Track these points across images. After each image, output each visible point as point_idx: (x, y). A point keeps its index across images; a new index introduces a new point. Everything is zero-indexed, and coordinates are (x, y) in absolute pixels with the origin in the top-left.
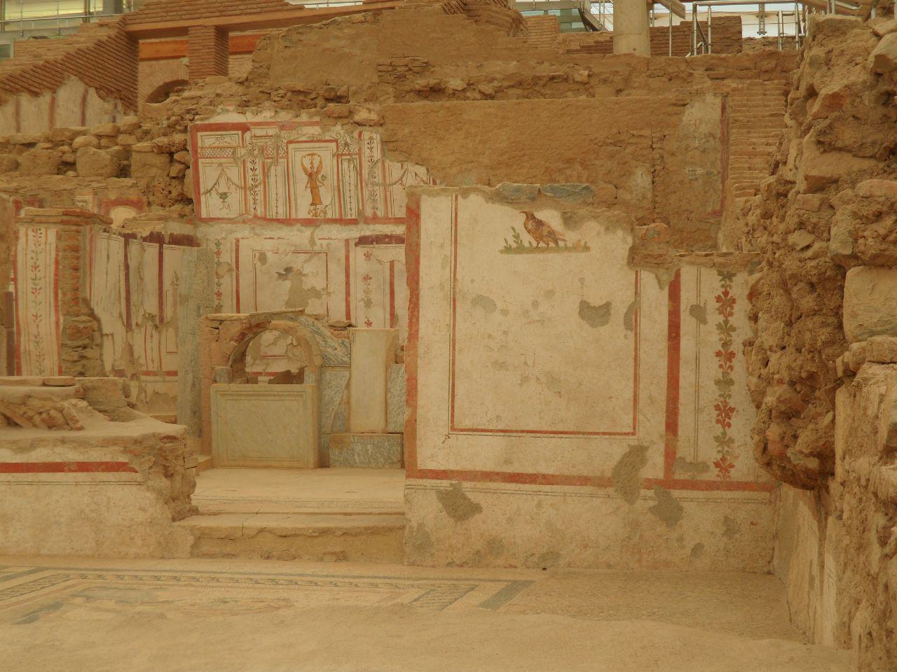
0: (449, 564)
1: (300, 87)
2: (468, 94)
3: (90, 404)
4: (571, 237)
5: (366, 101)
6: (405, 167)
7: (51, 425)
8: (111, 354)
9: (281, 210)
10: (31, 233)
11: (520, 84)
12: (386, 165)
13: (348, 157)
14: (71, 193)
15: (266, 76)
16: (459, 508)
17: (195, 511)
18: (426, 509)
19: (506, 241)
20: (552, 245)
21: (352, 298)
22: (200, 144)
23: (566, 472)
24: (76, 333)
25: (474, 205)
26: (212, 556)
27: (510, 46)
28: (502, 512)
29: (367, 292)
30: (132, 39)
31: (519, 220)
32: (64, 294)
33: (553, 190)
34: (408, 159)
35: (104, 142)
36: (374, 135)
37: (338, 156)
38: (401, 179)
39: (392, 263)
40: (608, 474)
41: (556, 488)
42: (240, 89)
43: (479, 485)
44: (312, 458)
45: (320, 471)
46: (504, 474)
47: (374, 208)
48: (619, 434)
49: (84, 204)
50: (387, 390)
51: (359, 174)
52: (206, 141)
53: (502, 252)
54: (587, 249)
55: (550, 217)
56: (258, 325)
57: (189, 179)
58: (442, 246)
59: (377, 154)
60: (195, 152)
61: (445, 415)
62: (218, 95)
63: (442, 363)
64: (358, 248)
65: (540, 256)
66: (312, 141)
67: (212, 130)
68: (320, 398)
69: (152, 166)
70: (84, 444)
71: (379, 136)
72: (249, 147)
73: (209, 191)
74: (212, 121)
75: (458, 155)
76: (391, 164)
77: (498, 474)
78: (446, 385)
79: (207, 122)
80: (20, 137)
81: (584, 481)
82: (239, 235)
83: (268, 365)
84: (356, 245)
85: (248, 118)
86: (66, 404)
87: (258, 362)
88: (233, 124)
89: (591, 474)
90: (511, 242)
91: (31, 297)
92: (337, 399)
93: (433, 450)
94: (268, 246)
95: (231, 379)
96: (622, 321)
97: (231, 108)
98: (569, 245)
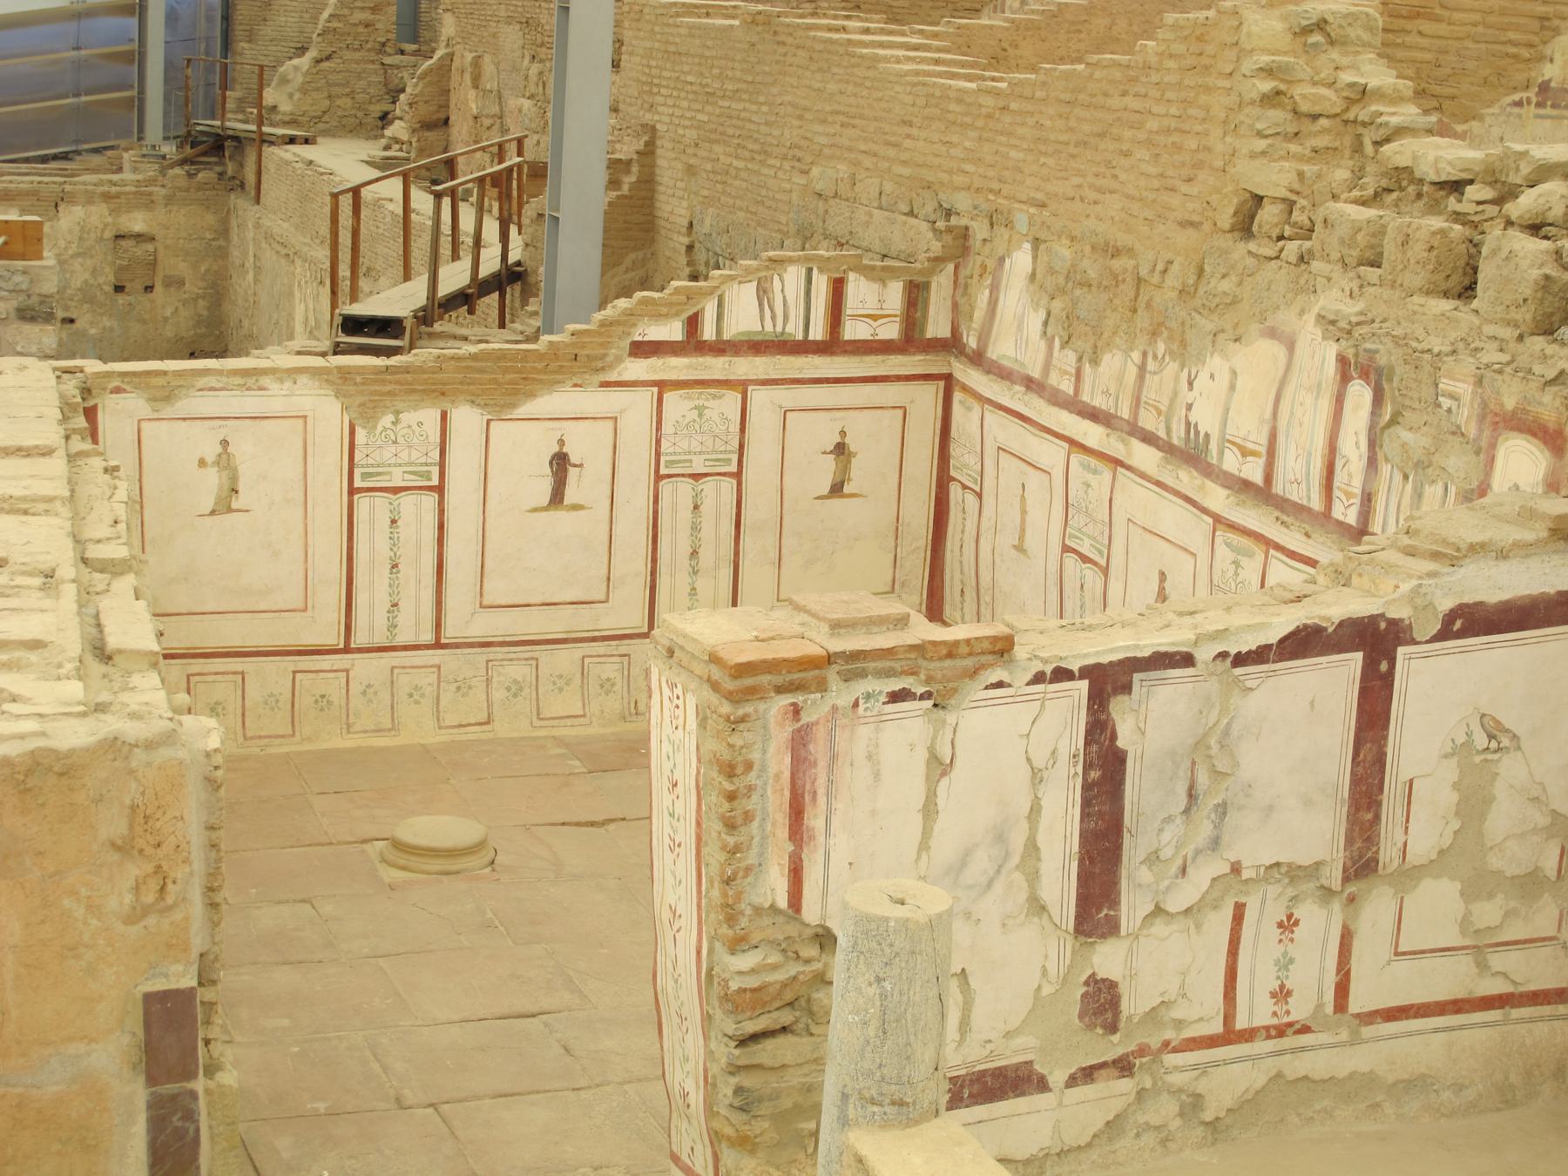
32: (711, 882)
49: (1454, 405)
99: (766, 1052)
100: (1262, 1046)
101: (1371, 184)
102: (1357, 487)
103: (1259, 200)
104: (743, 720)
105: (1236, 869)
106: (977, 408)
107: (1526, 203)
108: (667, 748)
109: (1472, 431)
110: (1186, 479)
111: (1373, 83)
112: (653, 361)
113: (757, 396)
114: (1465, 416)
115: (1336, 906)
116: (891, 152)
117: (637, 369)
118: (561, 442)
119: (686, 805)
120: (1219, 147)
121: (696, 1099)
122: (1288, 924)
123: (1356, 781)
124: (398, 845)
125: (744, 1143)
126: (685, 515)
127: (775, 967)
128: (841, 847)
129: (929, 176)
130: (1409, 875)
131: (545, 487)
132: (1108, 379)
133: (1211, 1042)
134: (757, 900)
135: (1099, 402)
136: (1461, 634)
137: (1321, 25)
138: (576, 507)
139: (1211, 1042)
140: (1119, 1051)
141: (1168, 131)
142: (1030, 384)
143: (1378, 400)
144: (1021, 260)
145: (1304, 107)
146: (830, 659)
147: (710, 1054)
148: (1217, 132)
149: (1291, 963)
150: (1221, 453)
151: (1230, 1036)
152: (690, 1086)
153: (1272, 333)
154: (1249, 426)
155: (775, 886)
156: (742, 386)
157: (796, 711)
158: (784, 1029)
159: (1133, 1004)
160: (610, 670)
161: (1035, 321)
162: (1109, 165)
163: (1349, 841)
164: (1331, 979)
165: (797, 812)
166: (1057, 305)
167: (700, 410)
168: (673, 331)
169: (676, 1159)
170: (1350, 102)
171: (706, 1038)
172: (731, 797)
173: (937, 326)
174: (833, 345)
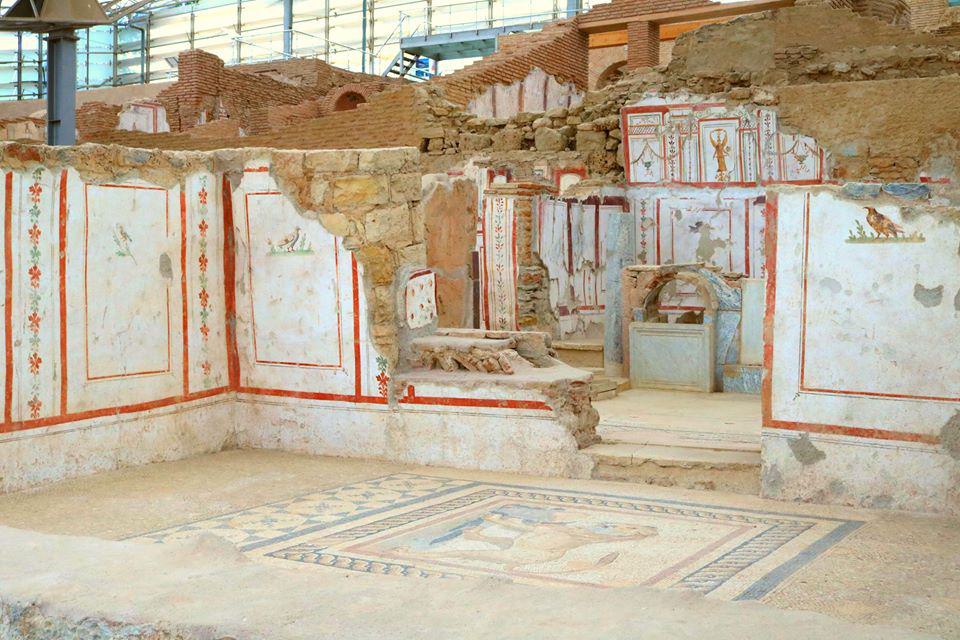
0: (797, 500)
1: (710, 73)
2: (852, 75)
3: (520, 353)
4: (908, 228)
5: (764, 84)
7: (490, 370)
8: (556, 295)
9: (693, 175)
10: (495, 203)
11: (898, 66)
12: (781, 137)
14: (531, 164)
15: (683, 66)
16: (807, 455)
17: (598, 440)
18: (778, 452)
19: (851, 232)
20: (891, 235)
21: (750, 248)
22: (629, 124)
23: (899, 430)
24: (529, 279)
25: (824, 201)
26: (608, 478)
27: (890, 33)
28: (843, 460)
30: (584, 34)
31: (862, 215)
32: (520, 249)
33: (893, 188)
34: (799, 132)
36: (771, 114)
37: (741, 130)
40: (937, 433)
41: (889, 442)
42: (662, 78)
43: (824, 436)
44: (708, 384)
45: (717, 395)
46: (845, 428)
48: (947, 399)
53: (847, 241)
54: (922, 239)
55: (890, 212)
56: (667, 276)
57: (621, 152)
58: (796, 236)
59: (773, 128)
61: (796, 377)
62: (644, 83)
63: (794, 333)
64: (756, 206)
65: (880, 245)
66: (720, 119)
68: (716, 335)
69: (592, 141)
70: (513, 386)
71: (774, 114)
74: (639, 105)
77: (840, 428)
78: (797, 353)
79: (635, 106)
80: (493, 121)
81: (916, 437)
82: (659, 196)
84: (755, 203)
85: (668, 101)
86: (501, 353)
88: (655, 107)
89: (921, 432)
90: (855, 233)
91: (496, 251)
92: (730, 337)
93: (786, 407)
94: (682, 205)
95: (646, 319)
96: (953, 302)
97: (653, 94)
98: (907, 236)
103: (427, 141)
121: (510, 318)
137: (434, 92)
141: (381, 128)
145: (437, 113)
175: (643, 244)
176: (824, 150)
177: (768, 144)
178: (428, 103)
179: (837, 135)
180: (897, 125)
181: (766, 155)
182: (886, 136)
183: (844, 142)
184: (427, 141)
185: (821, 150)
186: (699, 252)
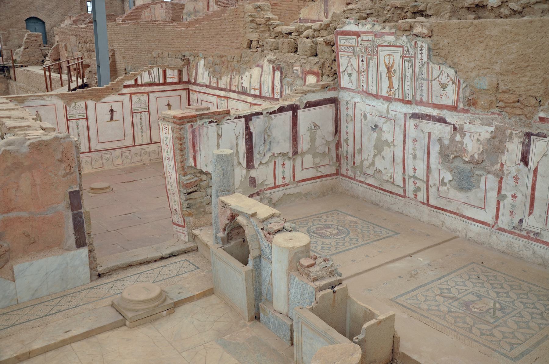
6: (441, 69)
12: (430, 66)
13: (409, 59)
21: (406, 151)
24: (185, 186)
29: (414, 149)
32: (178, 163)
34: (445, 63)
35: (316, 34)
36: (424, 44)
37: (403, 57)
38: (439, 77)
39: (430, 133)
47: (421, 95)
50: (289, 289)
51: (414, 71)
52: (342, 41)
59: (425, 58)
60: (337, 47)
64: (412, 120)
66: (390, 46)
67: (344, 35)
69: (325, 52)
72: (360, 47)
73: (344, 72)
75: (478, 63)
76: (433, 65)
82: (356, 100)
83: (366, 178)
84: (410, 118)
87: (362, 175)
91: (167, 161)
94: (368, 109)
97: (352, 21)
99: (193, 195)
100: (281, 188)
101: (273, 36)
102: (279, 90)
103: (251, 41)
104: (182, 129)
105: (274, 154)
106: (196, 94)
107: (305, 33)
108: (165, 139)
109: (301, 76)
110: (243, 97)
111: (270, 17)
112: (128, 89)
113: (151, 95)
114: (299, 73)
115: (291, 161)
116: (170, 46)
117: (125, 91)
118: (111, 107)
119: (171, 149)
120: (242, 32)
121: (178, 209)
122: (283, 165)
123: (293, 136)
124: (91, 189)
125: (190, 215)
126: (139, 120)
127: (193, 178)
128: (203, 153)
129: (179, 49)
130: (303, 154)
131: (109, 117)
132: (224, 82)
133: (272, 188)
134: (188, 165)
135: (222, 87)
136: (308, 107)
137: (259, 7)
138: (116, 120)
139: (272, 188)
140: (257, 191)
141: (231, 31)
142: (207, 86)
143: (281, 74)
144: (202, 63)
145: (258, 23)
146: (197, 116)
147: (181, 198)
148: (242, 29)
149: (285, 171)
150: (250, 91)
151: (276, 187)
152: (177, 207)
153: (258, 66)
154: (256, 85)
155: (191, 162)
156: (148, 93)
157: (192, 126)
158: (195, 191)
159: (258, 182)
160: (127, 154)
161: (206, 74)
162: (219, 40)
163: (293, 148)
164: (292, 175)
165: (194, 147)
166: (211, 69)
167: (139, 98)
168: (132, 82)
169: (174, 224)
170: (267, 21)
171: (180, 195)
172: (181, 144)
173: (185, 79)
174: (165, 83)
175: (347, 132)
176: (462, 81)
177: (421, 73)
178: (251, 16)
179: (473, 68)
180: (526, 64)
181: (419, 80)
182: (513, 73)
183: (478, 75)
184: (251, 41)
185: (459, 81)
186: (375, 147)
